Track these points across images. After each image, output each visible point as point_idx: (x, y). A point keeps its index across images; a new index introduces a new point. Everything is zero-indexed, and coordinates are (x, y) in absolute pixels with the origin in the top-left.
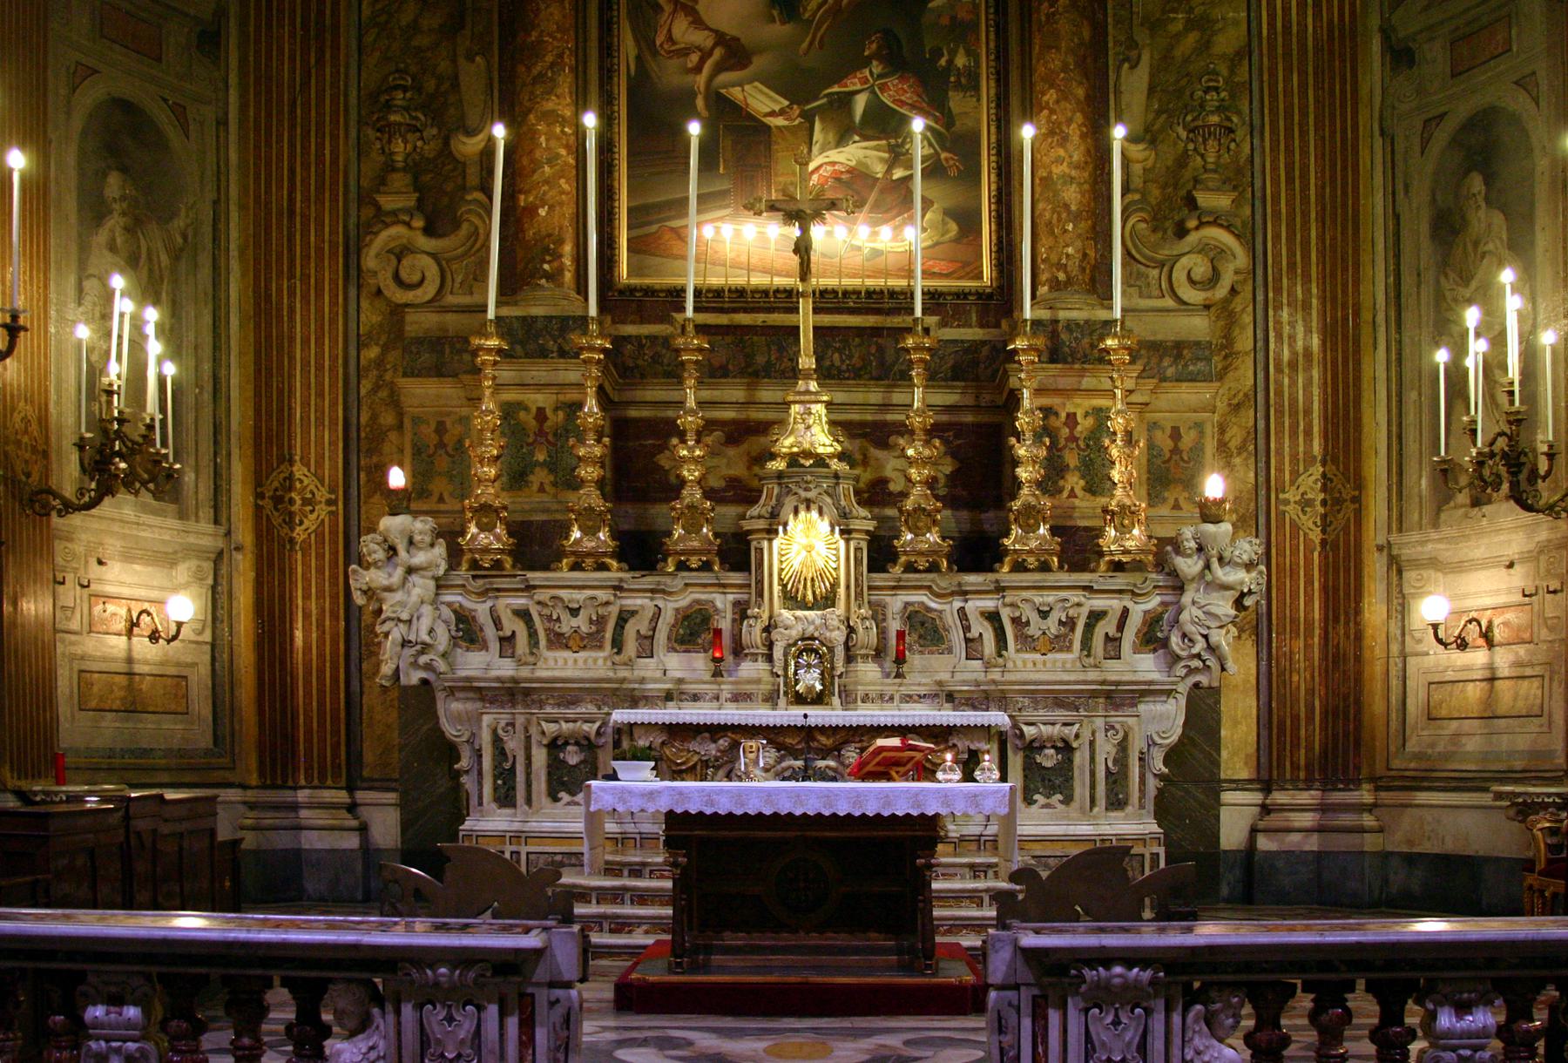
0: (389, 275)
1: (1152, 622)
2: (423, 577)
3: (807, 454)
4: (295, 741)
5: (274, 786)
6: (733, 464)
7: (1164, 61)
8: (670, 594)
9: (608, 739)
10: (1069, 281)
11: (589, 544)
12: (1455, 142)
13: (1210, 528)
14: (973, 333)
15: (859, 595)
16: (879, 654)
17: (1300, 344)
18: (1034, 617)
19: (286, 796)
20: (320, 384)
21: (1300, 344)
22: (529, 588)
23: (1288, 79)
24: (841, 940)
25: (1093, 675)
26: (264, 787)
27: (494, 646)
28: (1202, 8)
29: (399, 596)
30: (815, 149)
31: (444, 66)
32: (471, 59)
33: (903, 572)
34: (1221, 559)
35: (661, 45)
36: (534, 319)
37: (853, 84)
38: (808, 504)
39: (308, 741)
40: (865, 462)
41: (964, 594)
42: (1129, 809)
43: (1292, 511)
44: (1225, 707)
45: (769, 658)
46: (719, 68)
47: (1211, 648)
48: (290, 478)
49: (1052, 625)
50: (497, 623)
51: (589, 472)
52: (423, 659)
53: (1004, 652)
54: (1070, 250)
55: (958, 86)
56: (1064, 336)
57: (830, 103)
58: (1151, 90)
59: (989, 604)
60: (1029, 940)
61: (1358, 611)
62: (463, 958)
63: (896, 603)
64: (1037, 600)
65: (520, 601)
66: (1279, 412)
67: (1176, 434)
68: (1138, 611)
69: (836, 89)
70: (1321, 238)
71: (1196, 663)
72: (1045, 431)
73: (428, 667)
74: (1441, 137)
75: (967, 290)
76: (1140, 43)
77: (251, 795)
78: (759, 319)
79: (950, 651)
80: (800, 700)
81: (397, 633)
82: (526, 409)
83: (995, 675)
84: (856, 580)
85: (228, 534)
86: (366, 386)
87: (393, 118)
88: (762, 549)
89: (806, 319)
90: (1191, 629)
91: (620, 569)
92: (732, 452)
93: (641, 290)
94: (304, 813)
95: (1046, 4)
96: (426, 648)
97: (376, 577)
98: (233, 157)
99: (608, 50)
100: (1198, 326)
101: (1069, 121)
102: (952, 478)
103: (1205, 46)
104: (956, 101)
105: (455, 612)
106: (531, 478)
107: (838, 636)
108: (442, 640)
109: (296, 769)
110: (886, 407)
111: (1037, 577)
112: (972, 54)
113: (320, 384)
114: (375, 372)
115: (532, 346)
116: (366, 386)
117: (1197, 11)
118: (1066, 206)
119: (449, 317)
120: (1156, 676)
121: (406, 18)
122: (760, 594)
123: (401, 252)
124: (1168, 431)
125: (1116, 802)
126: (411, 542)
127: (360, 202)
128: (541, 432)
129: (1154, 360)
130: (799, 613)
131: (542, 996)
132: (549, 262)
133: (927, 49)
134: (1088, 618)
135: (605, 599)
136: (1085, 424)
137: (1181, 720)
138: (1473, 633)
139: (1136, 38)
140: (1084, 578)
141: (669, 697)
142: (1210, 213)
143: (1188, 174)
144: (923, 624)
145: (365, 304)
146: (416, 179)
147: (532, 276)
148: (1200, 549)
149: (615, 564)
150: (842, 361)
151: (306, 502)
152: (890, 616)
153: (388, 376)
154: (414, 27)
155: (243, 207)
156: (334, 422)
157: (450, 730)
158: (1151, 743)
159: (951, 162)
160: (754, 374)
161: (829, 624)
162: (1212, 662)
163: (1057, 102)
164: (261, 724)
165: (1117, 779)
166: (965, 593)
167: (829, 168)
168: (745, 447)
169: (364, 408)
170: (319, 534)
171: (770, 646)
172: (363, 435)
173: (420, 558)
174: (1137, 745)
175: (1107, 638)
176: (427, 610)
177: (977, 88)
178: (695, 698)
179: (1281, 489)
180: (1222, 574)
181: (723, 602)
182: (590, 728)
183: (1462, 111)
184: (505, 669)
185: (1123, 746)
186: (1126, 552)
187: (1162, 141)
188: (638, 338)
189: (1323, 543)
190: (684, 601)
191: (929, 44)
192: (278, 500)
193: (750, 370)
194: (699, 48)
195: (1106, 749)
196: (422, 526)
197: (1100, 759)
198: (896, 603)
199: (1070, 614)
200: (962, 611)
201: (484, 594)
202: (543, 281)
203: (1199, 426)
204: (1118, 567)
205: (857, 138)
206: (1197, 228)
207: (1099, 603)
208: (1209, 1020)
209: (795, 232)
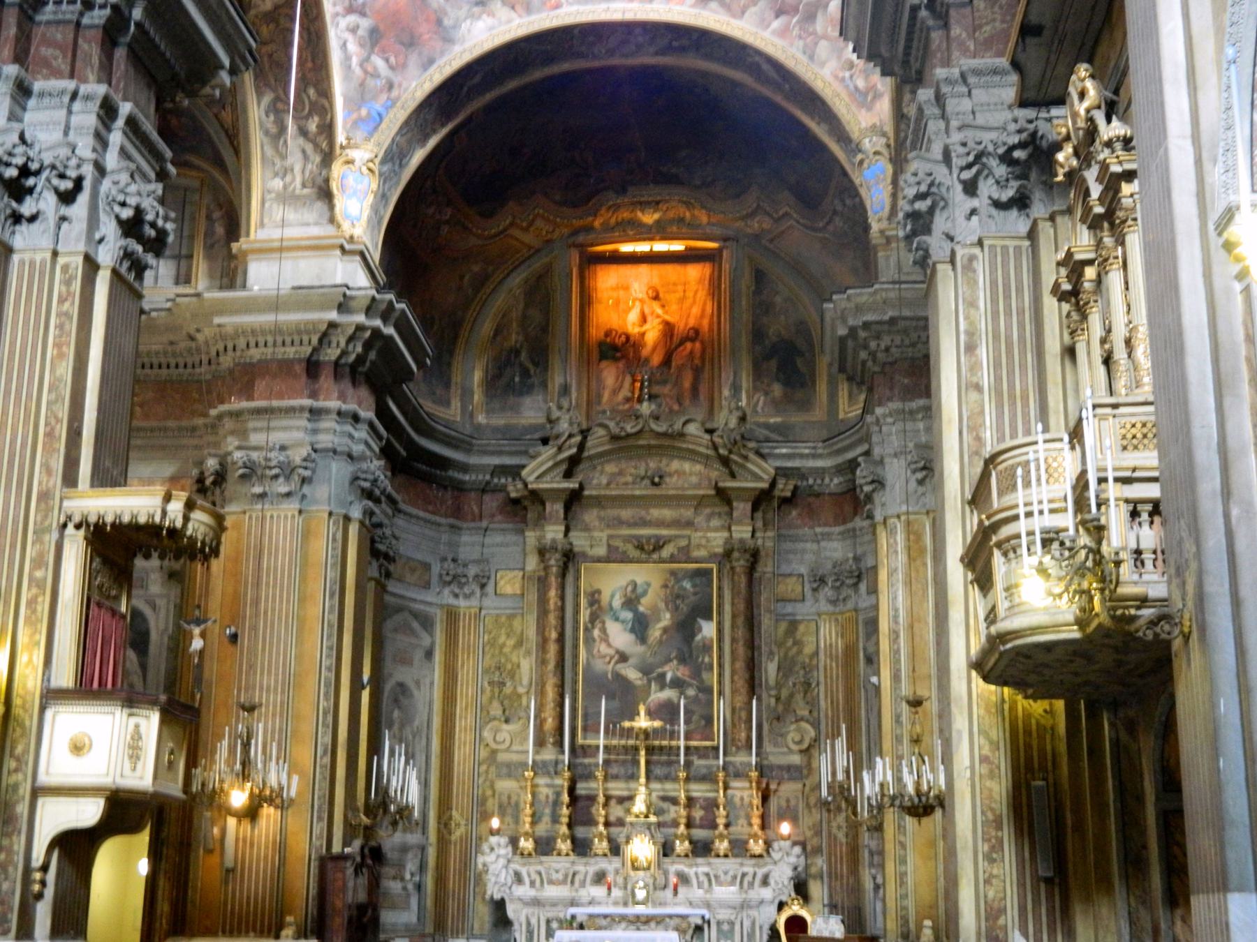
31: (515, 659)
37: (666, 668)
41: (697, 865)
43: (834, 831)
45: (625, 888)
50: (529, 875)
58: (779, 668)
59: (706, 869)
68: (761, 872)
81: (493, 879)
83: (708, 896)
100: (796, 759)
103: (800, 652)
108: (509, 881)
176: (504, 871)
178: (599, 903)
185: (753, 923)
195: (747, 924)
200: (696, 874)
201: (524, 865)
207: (746, 869)
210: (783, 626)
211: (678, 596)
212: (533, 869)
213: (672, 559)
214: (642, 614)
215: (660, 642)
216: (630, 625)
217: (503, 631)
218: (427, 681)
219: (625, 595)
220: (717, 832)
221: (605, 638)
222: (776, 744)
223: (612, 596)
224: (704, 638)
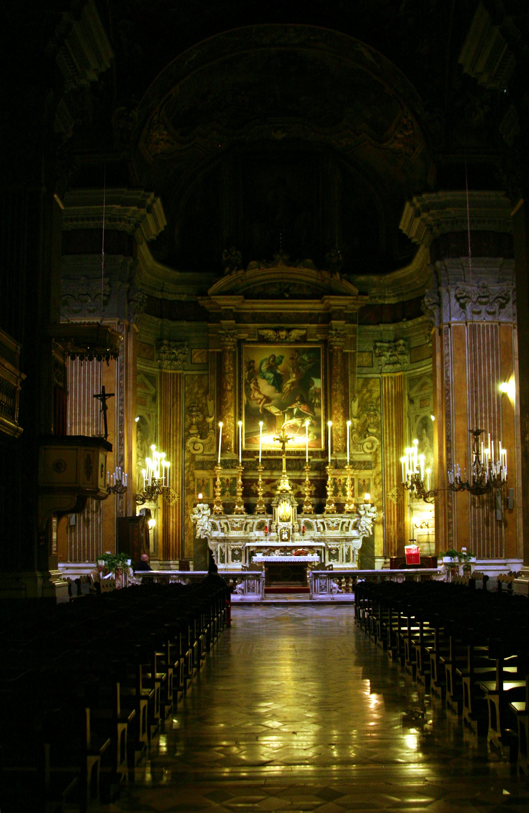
3: (284, 490)
4: (170, 550)
5: (165, 560)
6: (268, 488)
7: (362, 400)
9: (244, 549)
10: (340, 451)
11: (239, 509)
12: (421, 422)
14: (320, 460)
15: (295, 519)
17: (391, 461)
18: (331, 523)
20: (176, 472)
21: (391, 461)
22: (227, 518)
23: (389, 404)
24: (292, 582)
25: (343, 535)
26: (163, 560)
27: (220, 530)
29: (201, 520)
31: (204, 401)
32: (210, 401)
34: (368, 511)
37: (294, 406)
39: (173, 550)
40: (296, 488)
41: (316, 518)
43: (390, 497)
44: (376, 540)
45: (277, 532)
46: (265, 403)
47: (367, 529)
49: (335, 525)
50: (221, 525)
51: (240, 494)
52: (206, 533)
55: (316, 407)
56: (338, 463)
58: (359, 406)
59: (322, 520)
60: (314, 572)
61: (404, 519)
62: (253, 575)
63: (303, 520)
65: (226, 521)
66: (387, 476)
68: (352, 522)
69: (290, 407)
70: (396, 438)
71: (364, 532)
72: (335, 484)
73: (207, 535)
74: (419, 419)
77: (161, 562)
78: (273, 457)
80: (283, 540)
81: (201, 528)
83: (323, 535)
90: (363, 525)
92: (267, 486)
94: (171, 566)
96: (206, 531)
97: (196, 516)
98: (158, 422)
99: (240, 399)
100: (369, 458)
102: (315, 491)
103: (371, 396)
104: (316, 410)
107: (291, 528)
109: (170, 556)
110: (301, 476)
111: (331, 515)
112: (320, 400)
113: (176, 472)
118: (339, 435)
119: (205, 457)
121: (196, 390)
122: (275, 519)
125: (348, 561)
126: (203, 509)
128: (228, 484)
130: (283, 523)
131: (261, 579)
136: (342, 481)
137: (361, 544)
138: (424, 525)
140: (341, 515)
141: (256, 540)
148: (364, 509)
153: (191, 469)
155: (160, 434)
157: (211, 548)
158: (355, 549)
160: (272, 469)
161: (289, 525)
162: (367, 532)
164: (163, 546)
165: (348, 556)
168: (270, 485)
170: (176, 504)
171: (277, 529)
173: (205, 512)
174: (352, 549)
175: (346, 527)
177: (320, 407)
178: (262, 540)
179: (387, 492)
180: (368, 514)
181: (267, 520)
182: (240, 547)
183: (423, 415)
184: (222, 535)
185: (349, 549)
188: (247, 462)
189: (397, 504)
190: (259, 520)
191: (310, 397)
192: (167, 497)
194: (260, 399)
195: (345, 550)
196: (206, 506)
197: (344, 552)
198: (303, 520)
200: (316, 523)
201: (218, 519)
204: (349, 513)
207: (344, 520)
208: (333, 581)
210: (361, 381)
211: (300, 364)
212: (222, 521)
213: (297, 342)
214: (279, 374)
215: (290, 390)
216: (272, 381)
217: (197, 384)
218: (154, 414)
219: (269, 364)
221: (258, 389)
222: (357, 450)
223: (261, 364)
224: (316, 388)
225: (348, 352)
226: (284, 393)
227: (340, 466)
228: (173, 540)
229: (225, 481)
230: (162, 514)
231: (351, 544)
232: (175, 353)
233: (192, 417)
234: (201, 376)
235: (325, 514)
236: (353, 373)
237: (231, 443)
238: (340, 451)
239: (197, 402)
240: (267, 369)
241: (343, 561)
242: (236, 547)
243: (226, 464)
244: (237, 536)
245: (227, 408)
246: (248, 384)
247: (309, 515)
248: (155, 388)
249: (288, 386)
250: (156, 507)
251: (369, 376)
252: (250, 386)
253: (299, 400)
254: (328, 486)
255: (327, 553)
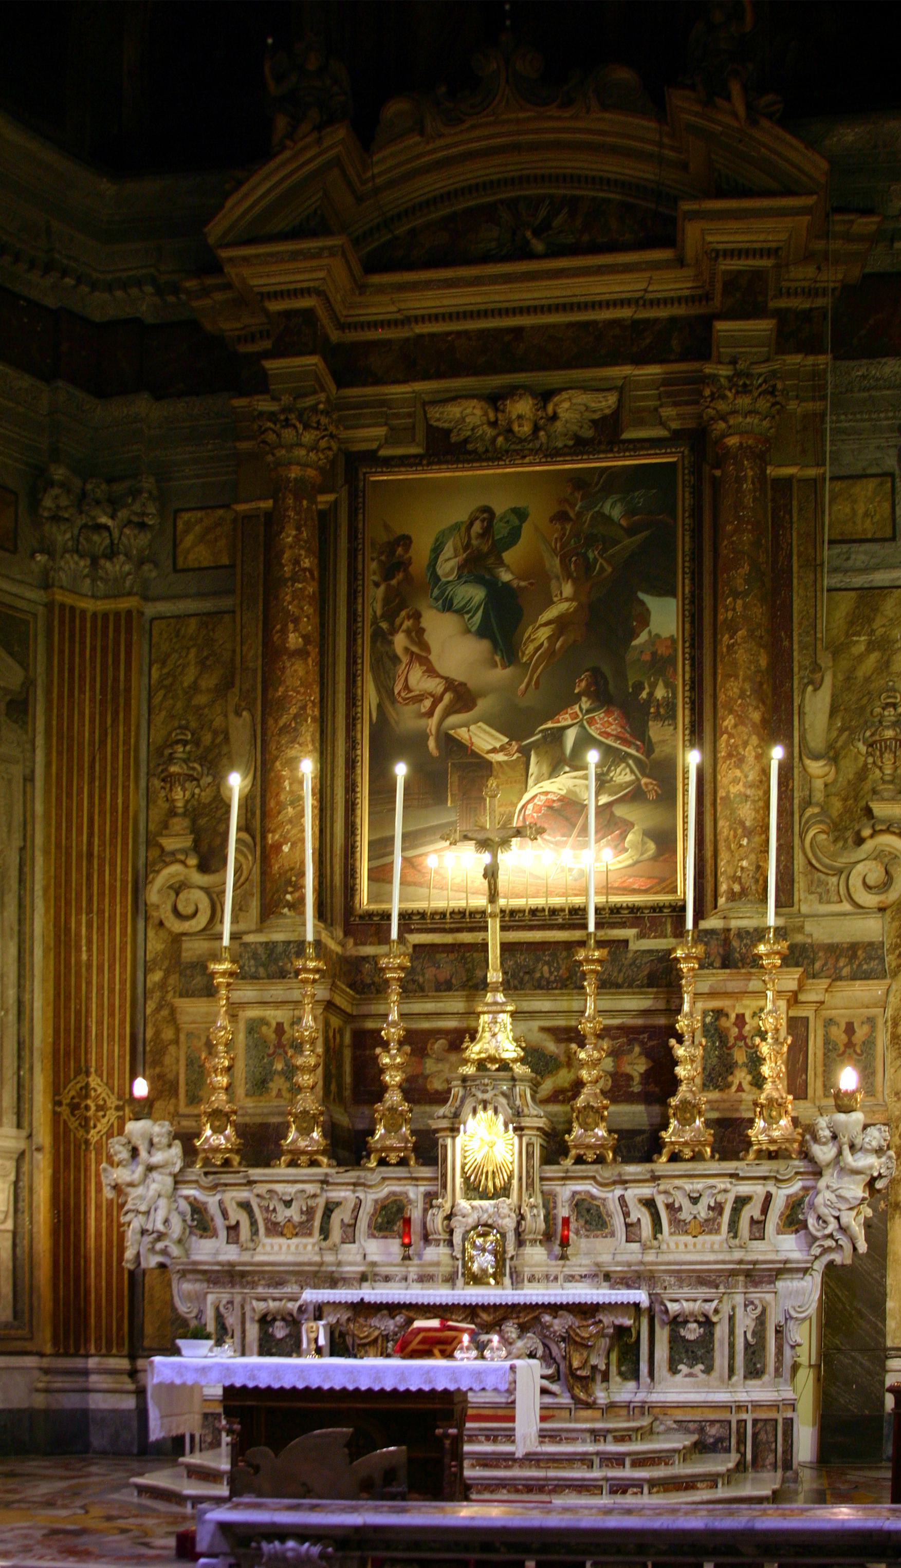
0: (169, 907)
1: (795, 1206)
2: (161, 1174)
3: (492, 1059)
8: (370, 1187)
10: (744, 892)
13: (842, 1117)
15: (530, 1185)
16: (548, 1237)
18: (686, 1203)
19: (78, 1363)
22: (250, 1183)
25: (738, 1255)
27: (223, 1234)
28: (883, 630)
29: (140, 1190)
30: (531, 781)
32: (238, 714)
33: (574, 1164)
34: (852, 1147)
35: (399, 693)
36: (275, 944)
38: (485, 1104)
42: (766, 1378)
45: (450, 1243)
47: (843, 1229)
48: (87, 1086)
49: (702, 1211)
53: (659, 1236)
54: (745, 863)
56: (735, 943)
57: (544, 738)
59: (646, 1191)
63: (565, 1192)
64: (688, 1187)
65: (244, 1194)
67: (850, 1029)
68: (781, 1195)
69: (549, 725)
71: (830, 1243)
73: (165, 1252)
75: (661, 904)
76: (823, 665)
79: (613, 1234)
81: (137, 1223)
82: (268, 1024)
83: (650, 1257)
84: (528, 1172)
85: (30, 1136)
86: (151, 1006)
87: (173, 769)
88: (446, 1146)
89: (494, 937)
90: (824, 1211)
91: (329, 1166)
93: (378, 914)
95: (727, 636)
96: (161, 1236)
97: (121, 1175)
98: (39, 808)
101: (745, 744)
105: (190, 1204)
106: (271, 1085)
107: (509, 1223)
114: (158, 994)
115: (273, 968)
116: (151, 1006)
117: (878, 633)
118: (742, 823)
120: (796, 1255)
122: (444, 1186)
123: (180, 887)
124: (843, 1026)
125: (754, 1372)
126: (151, 1144)
127: (148, 844)
129: (831, 962)
130: (477, 1203)
132: (291, 893)
133: (630, 683)
134: (735, 1202)
135: (312, 1192)
137: (816, 1295)
139: (819, 661)
140: (730, 1166)
141: (363, 1278)
142: (883, 822)
143: (867, 786)
144: (588, 1211)
145: (151, 934)
146: (194, 822)
147: (277, 906)
148: (835, 1137)
149: (325, 1160)
150: (551, 973)
151: (99, 1108)
152: (559, 1204)
154: (195, 688)
155: (46, 852)
156: (122, 1038)
157: (183, 1308)
158: (788, 1318)
159: (651, 787)
162: (844, 1241)
163: (735, 726)
165: (755, 1351)
166: (626, 1182)
167: (543, 798)
169: (150, 1025)
171: (451, 1232)
172: (148, 1049)
175: (753, 1221)
176: (163, 1203)
177: (674, 717)
178: (387, 1279)
181: (415, 1193)
184: (230, 1254)
185: (761, 1320)
186: (772, 1141)
187: (845, 757)
193: (470, 984)
194: (431, 695)
195: (745, 1323)
196: (159, 1129)
197: (739, 1332)
198: (565, 1192)
199: (718, 1199)
202: (286, 910)
203: (871, 1021)
204: (772, 1156)
205: (567, 769)
206: (872, 836)
207: (744, 1189)
209: (485, 858)
220: (674, 1101)
224: (655, 639)
225: (789, 479)
226: (527, 665)
227: (743, 958)
228: (98, 1274)
229: (269, 1033)
230: (49, 1172)
231: (769, 1297)
232: (106, 528)
233: (169, 780)
234: (209, 619)
235: (662, 1164)
236: (813, 565)
237: (302, 874)
238: (744, 892)
239: (193, 725)
240: (461, 568)
241: (732, 1371)
242: (272, 1305)
243: (276, 961)
244: (290, 1258)
245: (284, 729)
246: (382, 637)
247: (591, 1169)
248: (25, 667)
249: (543, 634)
250: (22, 1145)
251: (881, 578)
252: (391, 643)
253: (586, 693)
254: (680, 1040)
255: (663, 1335)
